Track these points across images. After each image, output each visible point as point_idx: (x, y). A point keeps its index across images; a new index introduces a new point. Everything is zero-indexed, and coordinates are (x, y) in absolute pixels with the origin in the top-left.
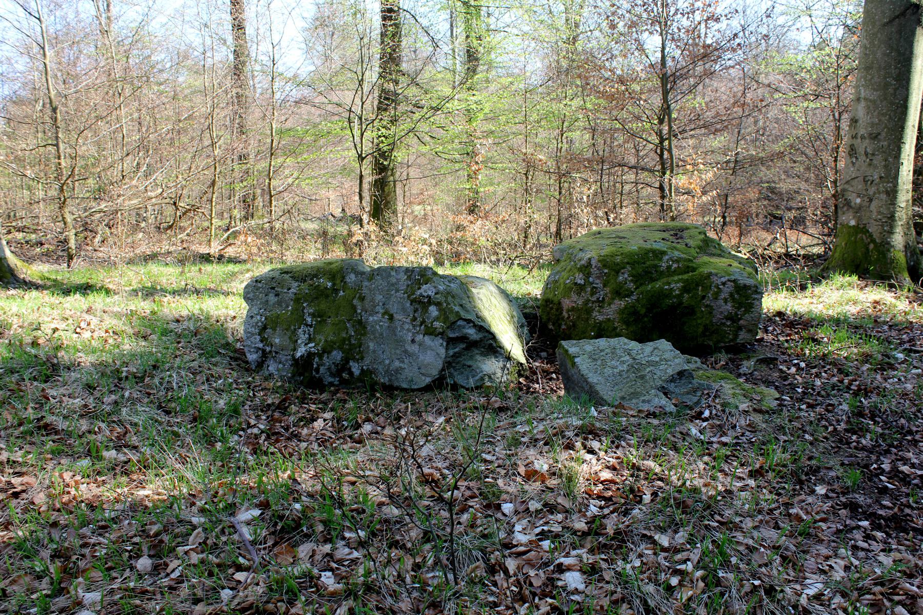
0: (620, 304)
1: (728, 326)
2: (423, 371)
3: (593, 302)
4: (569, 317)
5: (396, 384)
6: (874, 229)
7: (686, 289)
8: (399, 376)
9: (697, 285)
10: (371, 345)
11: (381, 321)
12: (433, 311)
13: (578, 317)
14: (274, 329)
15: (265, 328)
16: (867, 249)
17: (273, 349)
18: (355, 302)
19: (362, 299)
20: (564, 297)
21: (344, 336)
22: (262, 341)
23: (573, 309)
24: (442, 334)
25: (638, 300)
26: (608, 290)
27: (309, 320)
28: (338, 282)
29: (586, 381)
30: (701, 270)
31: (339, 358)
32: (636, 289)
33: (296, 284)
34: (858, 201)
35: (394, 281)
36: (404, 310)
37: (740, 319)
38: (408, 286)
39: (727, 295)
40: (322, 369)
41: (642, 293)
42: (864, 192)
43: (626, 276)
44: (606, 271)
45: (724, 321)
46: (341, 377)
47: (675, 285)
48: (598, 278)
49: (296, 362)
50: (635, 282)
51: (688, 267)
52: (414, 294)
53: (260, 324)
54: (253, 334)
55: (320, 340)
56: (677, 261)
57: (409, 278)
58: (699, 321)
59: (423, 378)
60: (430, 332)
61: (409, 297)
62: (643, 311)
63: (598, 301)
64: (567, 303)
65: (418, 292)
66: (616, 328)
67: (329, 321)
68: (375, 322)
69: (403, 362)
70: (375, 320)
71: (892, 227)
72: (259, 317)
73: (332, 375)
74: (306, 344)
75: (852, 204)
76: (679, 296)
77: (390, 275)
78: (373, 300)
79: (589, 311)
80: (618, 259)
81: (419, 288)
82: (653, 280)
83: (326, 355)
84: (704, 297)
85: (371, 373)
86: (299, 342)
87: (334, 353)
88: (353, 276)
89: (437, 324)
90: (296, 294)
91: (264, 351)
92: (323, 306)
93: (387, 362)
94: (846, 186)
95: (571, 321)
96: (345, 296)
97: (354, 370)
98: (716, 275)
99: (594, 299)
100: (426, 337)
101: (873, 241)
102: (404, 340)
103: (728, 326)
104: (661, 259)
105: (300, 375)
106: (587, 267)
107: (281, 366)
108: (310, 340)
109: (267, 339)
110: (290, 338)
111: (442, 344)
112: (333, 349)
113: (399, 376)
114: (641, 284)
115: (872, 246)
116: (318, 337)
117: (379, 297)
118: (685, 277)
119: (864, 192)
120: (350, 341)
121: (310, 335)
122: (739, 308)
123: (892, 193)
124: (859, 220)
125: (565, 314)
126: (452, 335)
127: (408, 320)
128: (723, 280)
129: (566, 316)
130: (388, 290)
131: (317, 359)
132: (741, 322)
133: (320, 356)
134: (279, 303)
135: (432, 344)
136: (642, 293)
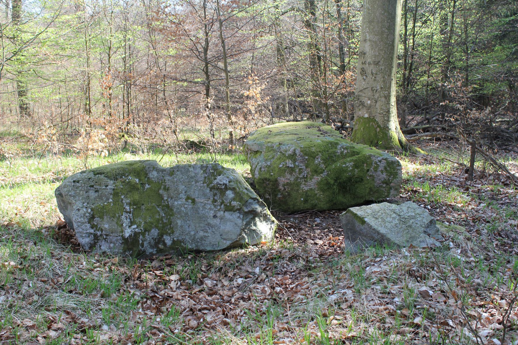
0: (317, 178)
1: (384, 188)
2: (225, 237)
3: (301, 178)
4: (285, 189)
5: (201, 248)
6: (379, 119)
7: (356, 166)
8: (203, 242)
9: (363, 163)
10: (179, 222)
11: (185, 204)
12: (230, 194)
13: (292, 189)
14: (102, 217)
15: (93, 217)
16: (376, 131)
17: (104, 232)
18: (161, 192)
19: (167, 189)
20: (280, 176)
21: (157, 217)
22: (92, 228)
23: (288, 184)
24: (238, 210)
25: (328, 175)
26: (309, 170)
27: (128, 208)
28: (143, 178)
29: (378, 233)
30: (364, 153)
31: (156, 234)
32: (326, 168)
33: (112, 182)
34: (369, 102)
35: (193, 175)
36: (204, 195)
37: (391, 183)
38: (205, 178)
39: (383, 168)
40: (145, 244)
41: (330, 170)
42: (372, 97)
43: (319, 160)
44: (307, 157)
45: (381, 185)
46: (158, 248)
47: (349, 164)
48: (302, 162)
49: (125, 241)
50: (324, 163)
51: (354, 152)
52: (211, 183)
53: (87, 215)
54: (83, 223)
55: (141, 223)
56: (346, 148)
57: (205, 172)
58: (366, 186)
59: (225, 242)
60: (229, 209)
61: (208, 185)
62: (332, 182)
63: (304, 177)
64: (282, 180)
65: (215, 182)
66: (316, 194)
67: (143, 207)
68: (180, 205)
69: (207, 232)
70: (179, 203)
71: (389, 117)
72: (85, 209)
73: (152, 247)
74: (129, 227)
75: (365, 104)
76: (353, 170)
77: (188, 171)
78: (176, 190)
79: (298, 185)
80: (313, 149)
81: (215, 179)
82: (334, 161)
83: (147, 233)
84: (368, 171)
85: (181, 242)
86: (124, 225)
87: (153, 230)
88: (155, 173)
89: (234, 203)
90: (114, 189)
91: (95, 236)
92: (136, 197)
93: (192, 233)
94: (360, 93)
95: (287, 192)
96: (150, 188)
97: (166, 241)
98: (374, 156)
99: (301, 176)
100: (226, 213)
101: (379, 126)
102: (207, 217)
103: (384, 188)
104: (336, 148)
105: (129, 249)
106: (293, 155)
107: (112, 245)
108: (132, 223)
109: (96, 226)
110: (117, 223)
111: (239, 217)
112: (152, 228)
113: (203, 242)
114: (328, 165)
115: (378, 129)
116: (138, 220)
117: (182, 187)
118: (354, 158)
119: (372, 97)
120: (163, 221)
121: (130, 219)
122: (390, 176)
123: (388, 97)
124: (370, 113)
125: (281, 187)
126: (246, 210)
127: (210, 202)
128: (379, 159)
129: (283, 189)
130: (189, 182)
131: (141, 237)
132: (392, 184)
133: (143, 234)
134: (100, 197)
135: (231, 217)
136: (330, 170)
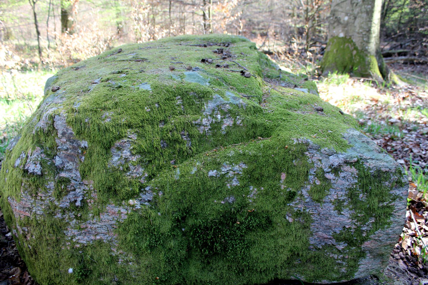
0: (117, 212)
6: (356, 40)
7: (252, 177)
9: (277, 170)
16: (352, 54)
25: (154, 203)
30: (284, 135)
32: (150, 178)
34: (346, 18)
37: (363, 240)
39: (342, 195)
42: (351, 12)
43: (126, 153)
45: (330, 242)
48: (70, 157)
51: (254, 126)
56: (232, 114)
58: (281, 242)
71: (369, 38)
75: (342, 21)
76: (241, 190)
79: (58, 229)
80: (108, 118)
82: (184, 156)
84: (291, 196)
94: (337, 8)
99: (65, 203)
101: (356, 48)
104: (199, 110)
106: (48, 134)
114: (160, 168)
115: (355, 52)
118: (251, 148)
119: (351, 12)
122: (364, 221)
123: (370, 13)
124: (346, 32)
128: (335, 160)
132: (367, 244)
